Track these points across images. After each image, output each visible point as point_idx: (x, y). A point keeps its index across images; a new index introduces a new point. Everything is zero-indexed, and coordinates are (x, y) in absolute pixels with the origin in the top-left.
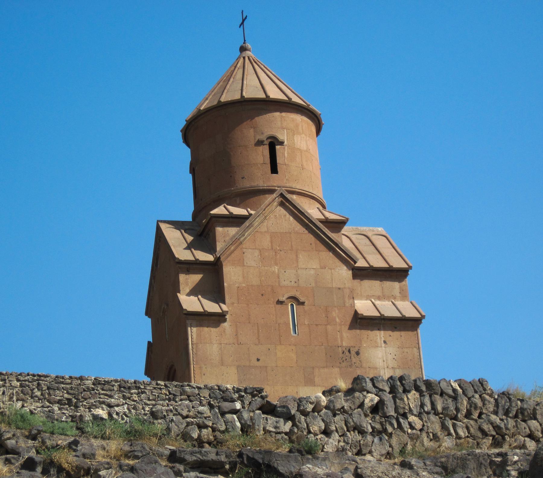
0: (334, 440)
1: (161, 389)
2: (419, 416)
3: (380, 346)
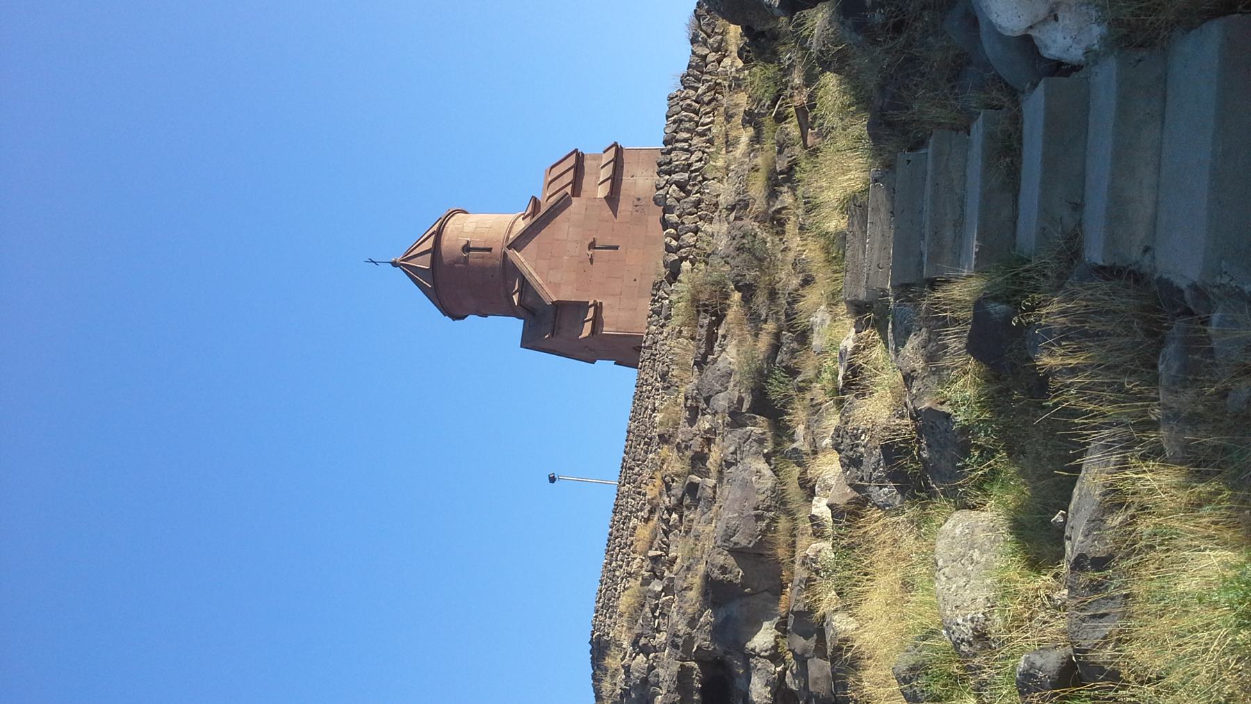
0: (703, 226)
1: (645, 366)
2: (692, 153)
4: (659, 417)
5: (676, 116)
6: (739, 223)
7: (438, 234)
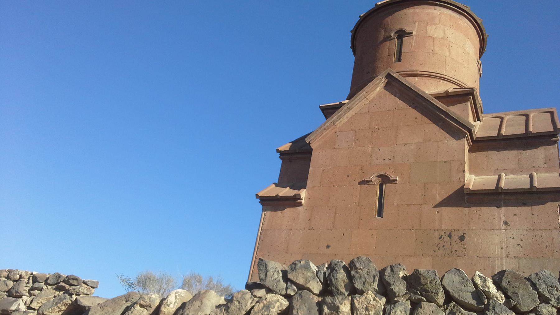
3: (497, 229)
5: (500, 298)
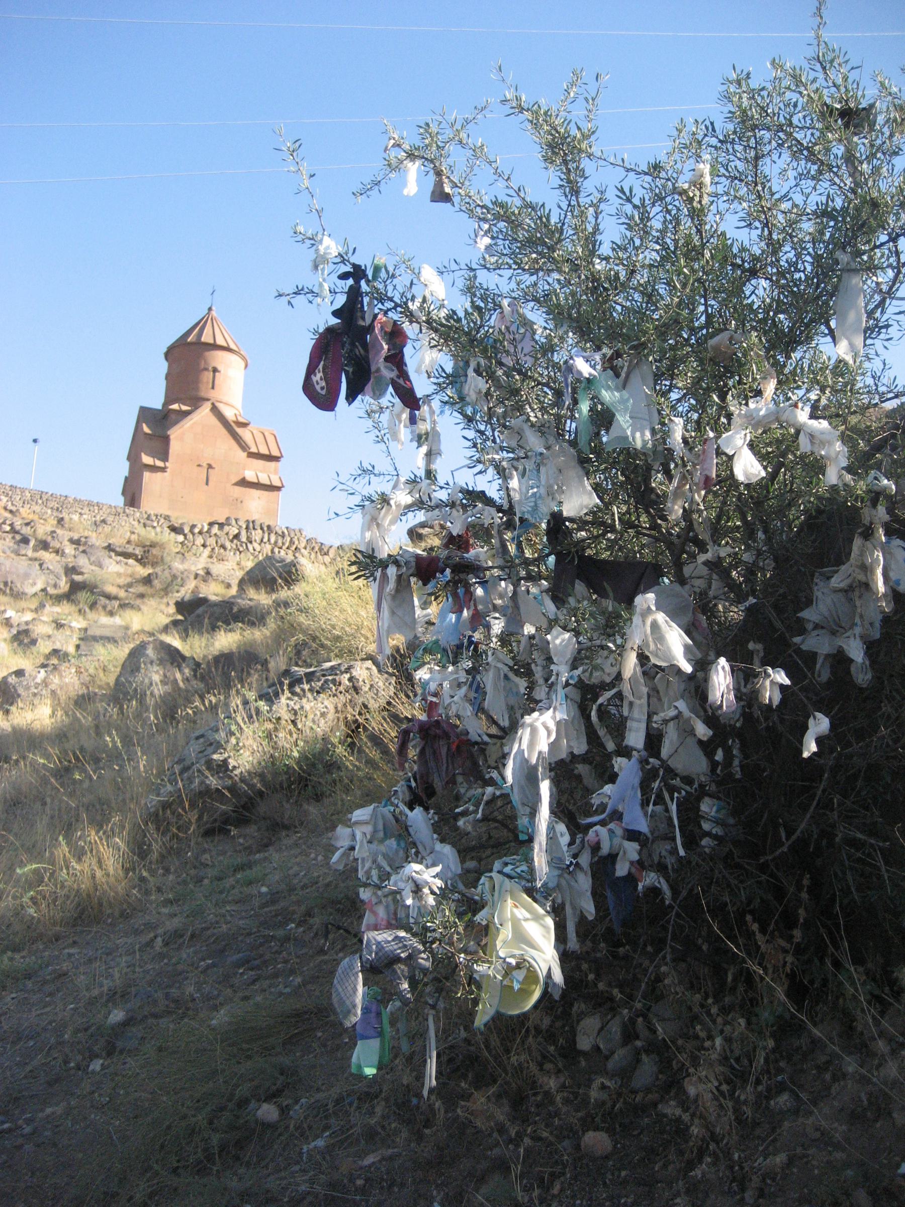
4: (76, 517)
6: (192, 577)
7: (227, 349)
